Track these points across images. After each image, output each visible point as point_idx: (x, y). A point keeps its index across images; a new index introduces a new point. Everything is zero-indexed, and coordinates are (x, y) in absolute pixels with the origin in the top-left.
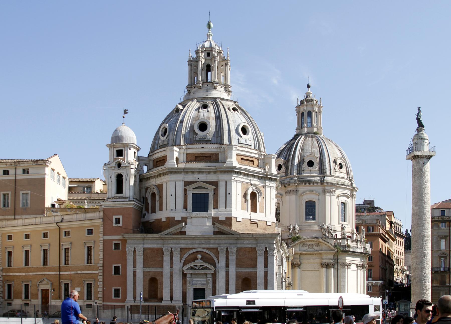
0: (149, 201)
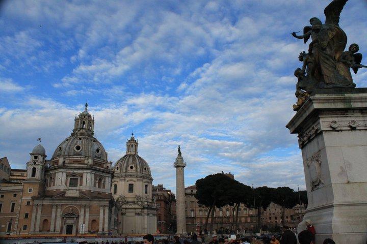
0: (49, 181)
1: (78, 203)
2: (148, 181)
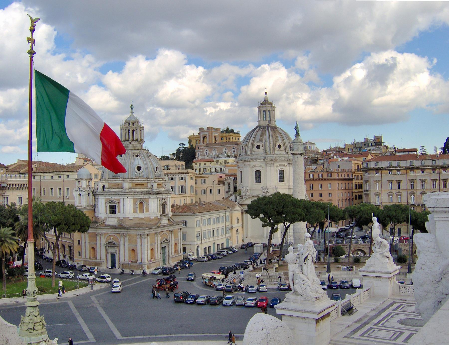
1: (118, 231)
2: (286, 163)
